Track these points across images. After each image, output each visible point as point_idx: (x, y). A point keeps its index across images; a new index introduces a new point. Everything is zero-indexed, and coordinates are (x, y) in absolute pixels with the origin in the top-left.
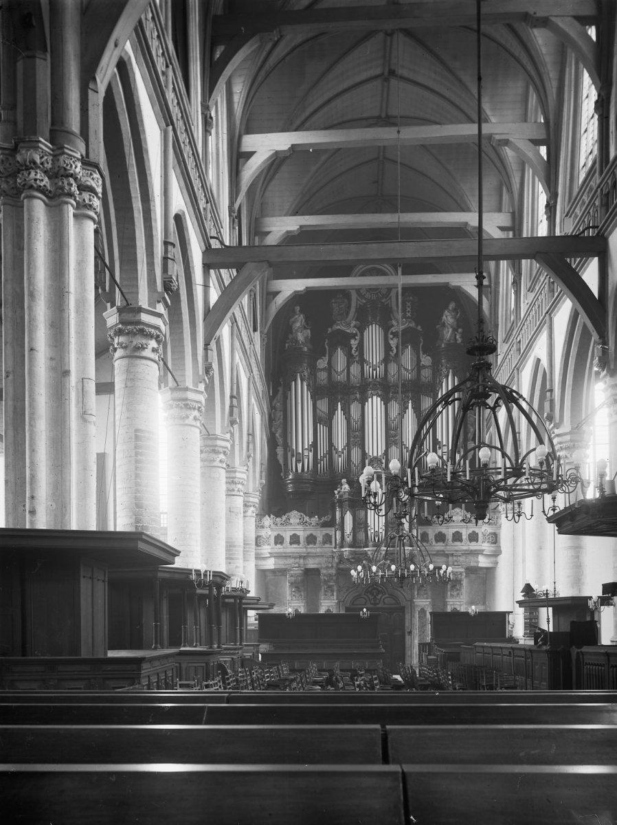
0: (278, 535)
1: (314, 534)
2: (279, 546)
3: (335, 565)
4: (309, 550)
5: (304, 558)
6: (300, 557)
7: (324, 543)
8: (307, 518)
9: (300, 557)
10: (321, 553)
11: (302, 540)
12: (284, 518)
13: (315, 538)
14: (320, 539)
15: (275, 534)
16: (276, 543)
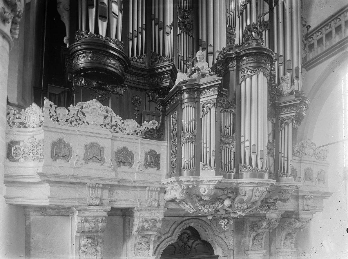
0: (60, 141)
1: (130, 149)
2: (60, 162)
3: (162, 204)
4: (121, 176)
5: (111, 188)
6: (105, 187)
7: (148, 165)
8: (117, 119)
9: (105, 187)
10: (143, 182)
11: (108, 156)
12: (74, 108)
13: (131, 155)
14: (139, 158)
15: (55, 137)
16: (55, 156)
